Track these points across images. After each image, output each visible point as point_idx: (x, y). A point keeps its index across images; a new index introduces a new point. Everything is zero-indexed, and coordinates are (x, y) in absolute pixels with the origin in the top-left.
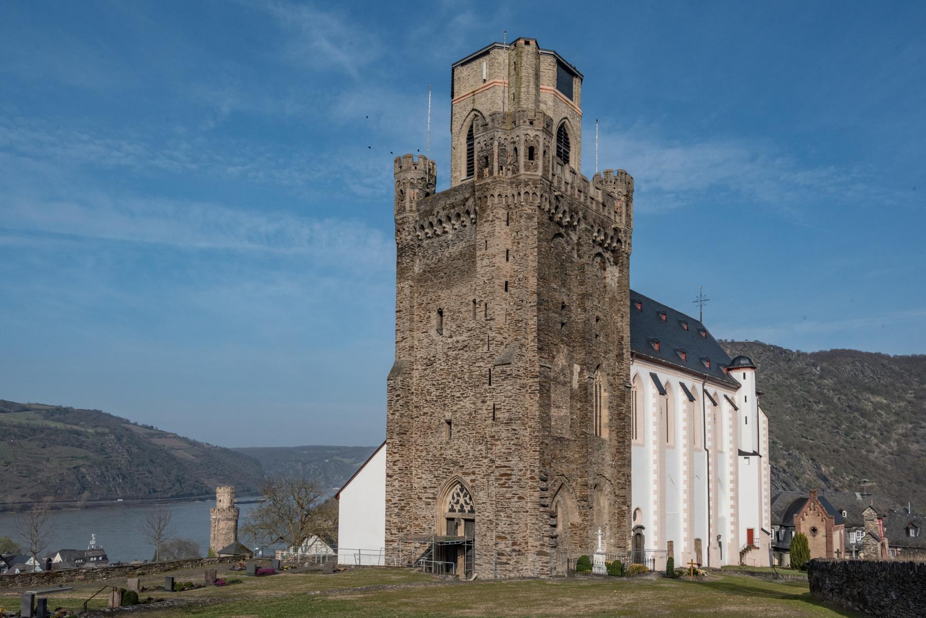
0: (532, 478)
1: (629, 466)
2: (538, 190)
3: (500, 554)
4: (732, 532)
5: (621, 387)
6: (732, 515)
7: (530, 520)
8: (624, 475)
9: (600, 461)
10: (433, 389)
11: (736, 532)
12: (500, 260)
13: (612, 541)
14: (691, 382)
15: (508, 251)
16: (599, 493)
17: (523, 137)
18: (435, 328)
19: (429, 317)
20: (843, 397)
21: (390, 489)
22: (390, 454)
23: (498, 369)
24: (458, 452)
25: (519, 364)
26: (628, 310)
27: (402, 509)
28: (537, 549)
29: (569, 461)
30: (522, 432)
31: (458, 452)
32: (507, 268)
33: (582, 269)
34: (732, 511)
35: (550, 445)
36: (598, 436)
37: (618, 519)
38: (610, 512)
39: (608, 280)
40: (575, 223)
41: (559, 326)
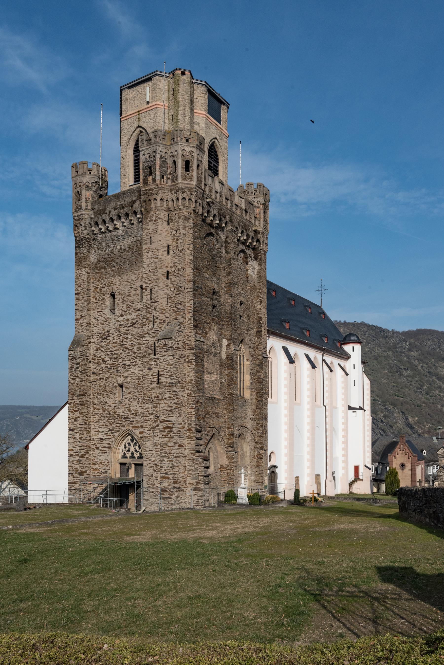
0: (189, 430)
1: (266, 419)
2: (194, 196)
3: (164, 491)
4: (343, 468)
5: (260, 357)
6: (343, 455)
7: (188, 463)
8: (262, 426)
9: (243, 415)
10: (107, 359)
11: (346, 468)
12: (162, 253)
13: (253, 478)
14: (313, 354)
15: (168, 246)
16: (243, 441)
17: (180, 152)
18: (109, 308)
20: (425, 365)
21: (72, 440)
22: (72, 412)
23: (162, 342)
24: (129, 410)
25: (179, 339)
26: (265, 297)
27: (83, 456)
28: (194, 486)
29: (219, 416)
30: (181, 393)
32: (168, 260)
33: (229, 262)
34: (343, 452)
35: (204, 403)
36: (241, 396)
37: (257, 461)
38: (250, 456)
39: (250, 272)
40: (224, 225)
41: (211, 308)
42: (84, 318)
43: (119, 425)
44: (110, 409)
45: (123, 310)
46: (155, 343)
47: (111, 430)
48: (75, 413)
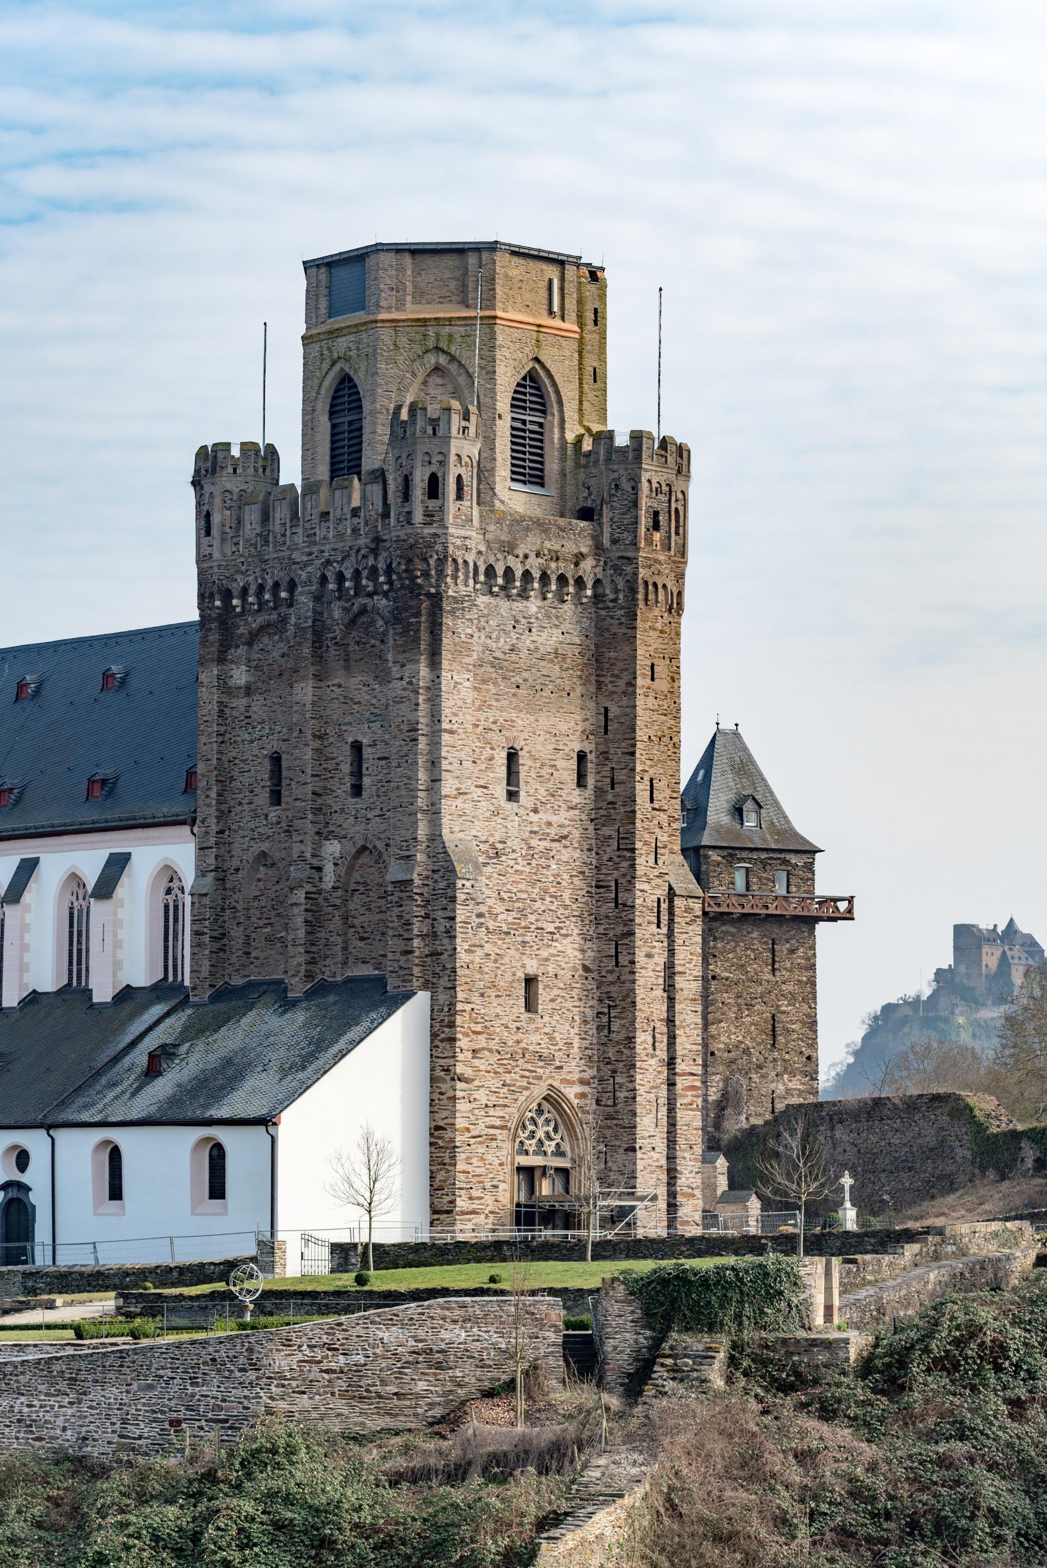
10: (499, 908)
19: (492, 759)
24: (551, 1039)
31: (551, 1039)
42: (466, 797)
43: (527, 1074)
44: (506, 1034)
45: (539, 797)
46: (659, 899)
47: (509, 1085)
48: (474, 1037)
